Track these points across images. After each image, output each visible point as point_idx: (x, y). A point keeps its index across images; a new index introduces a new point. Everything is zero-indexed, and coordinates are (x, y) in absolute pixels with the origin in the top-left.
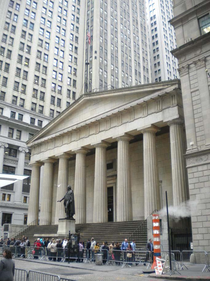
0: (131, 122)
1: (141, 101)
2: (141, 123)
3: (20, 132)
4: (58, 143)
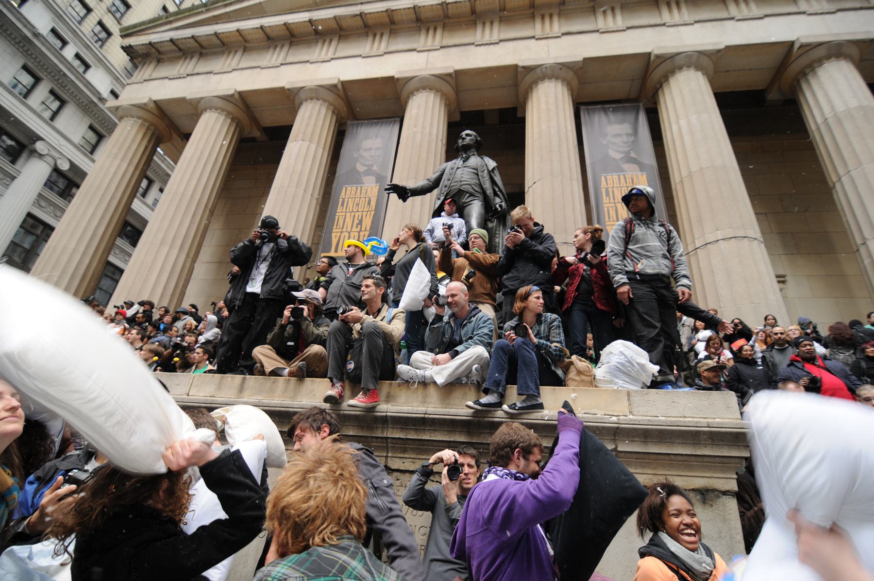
3: (63, 103)
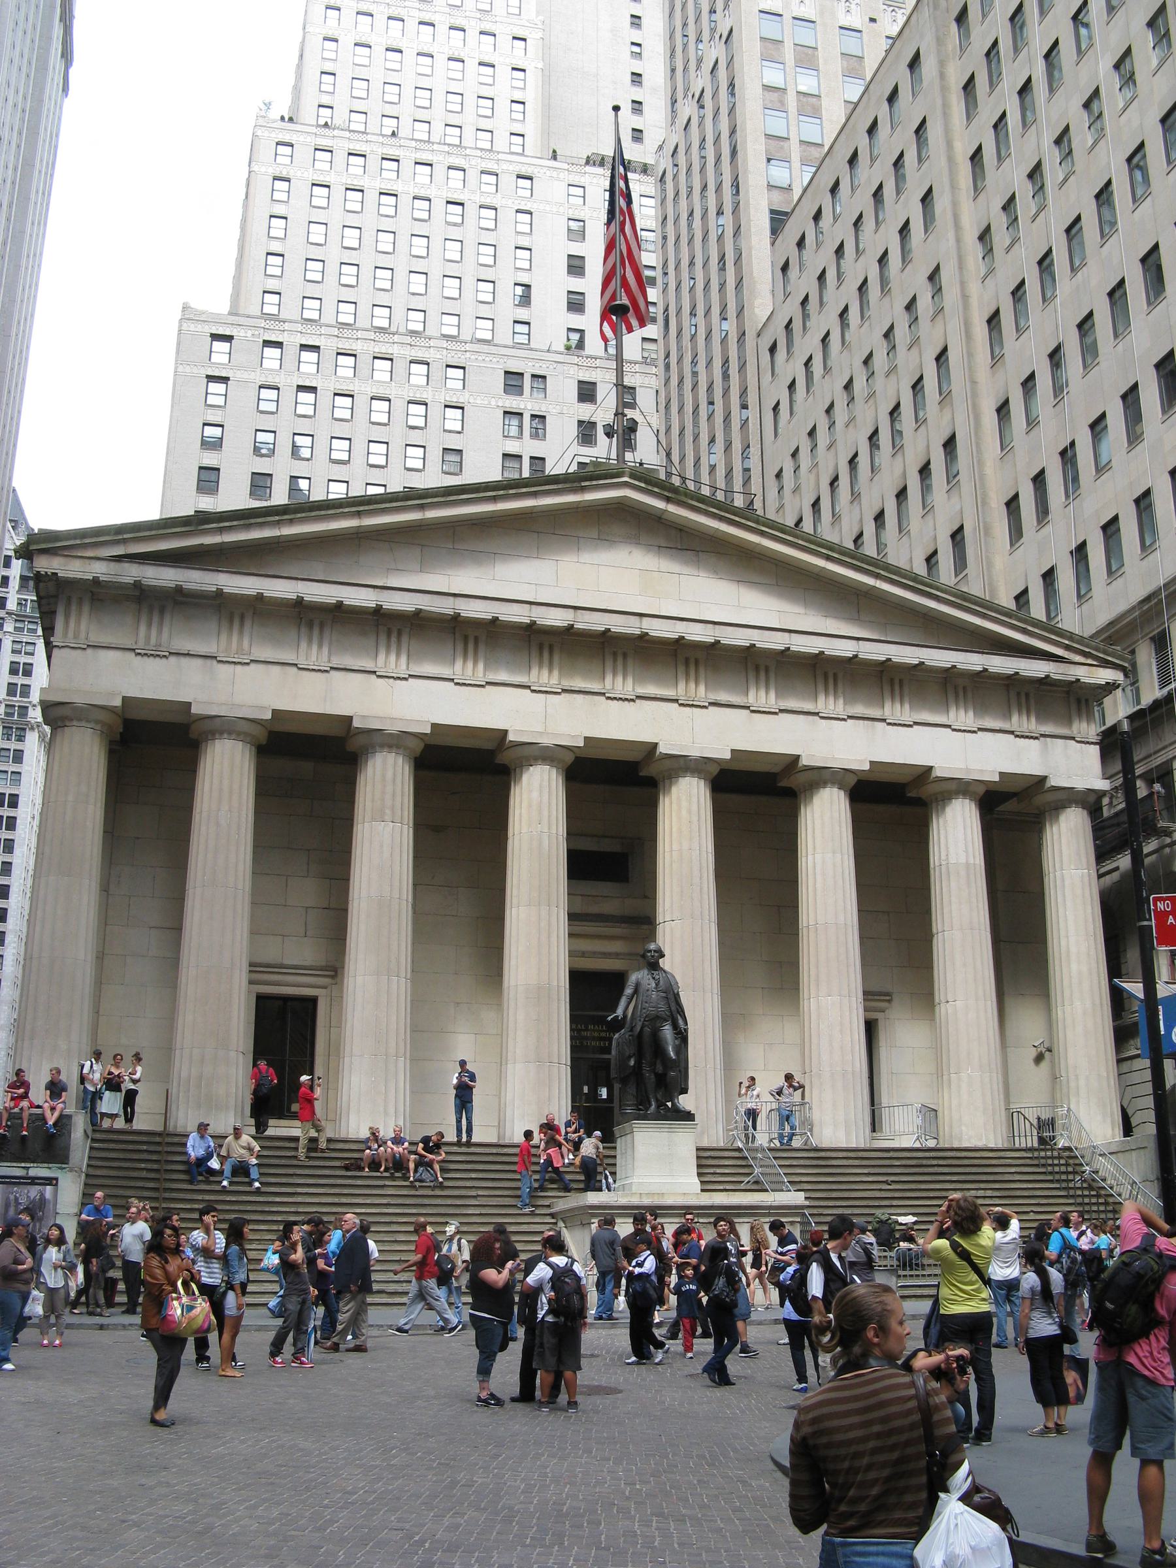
0: (900, 728)
1: (972, 661)
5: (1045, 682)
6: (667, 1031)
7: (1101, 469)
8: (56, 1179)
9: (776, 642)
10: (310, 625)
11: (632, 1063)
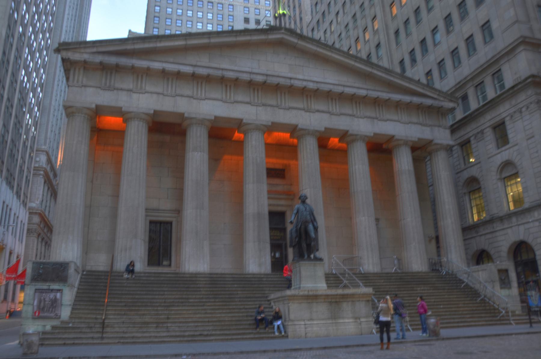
1: (407, 98)
2: (402, 128)
4: (187, 89)
5: (430, 107)
6: (311, 227)
7: (435, 45)
8: (62, 290)
9: (340, 89)
10: (168, 79)
11: (297, 240)
